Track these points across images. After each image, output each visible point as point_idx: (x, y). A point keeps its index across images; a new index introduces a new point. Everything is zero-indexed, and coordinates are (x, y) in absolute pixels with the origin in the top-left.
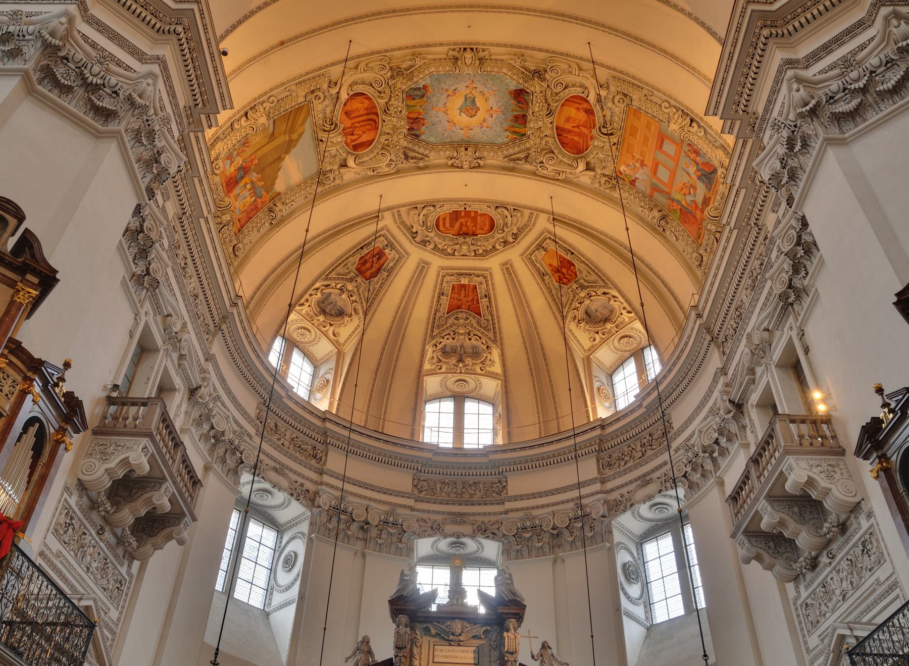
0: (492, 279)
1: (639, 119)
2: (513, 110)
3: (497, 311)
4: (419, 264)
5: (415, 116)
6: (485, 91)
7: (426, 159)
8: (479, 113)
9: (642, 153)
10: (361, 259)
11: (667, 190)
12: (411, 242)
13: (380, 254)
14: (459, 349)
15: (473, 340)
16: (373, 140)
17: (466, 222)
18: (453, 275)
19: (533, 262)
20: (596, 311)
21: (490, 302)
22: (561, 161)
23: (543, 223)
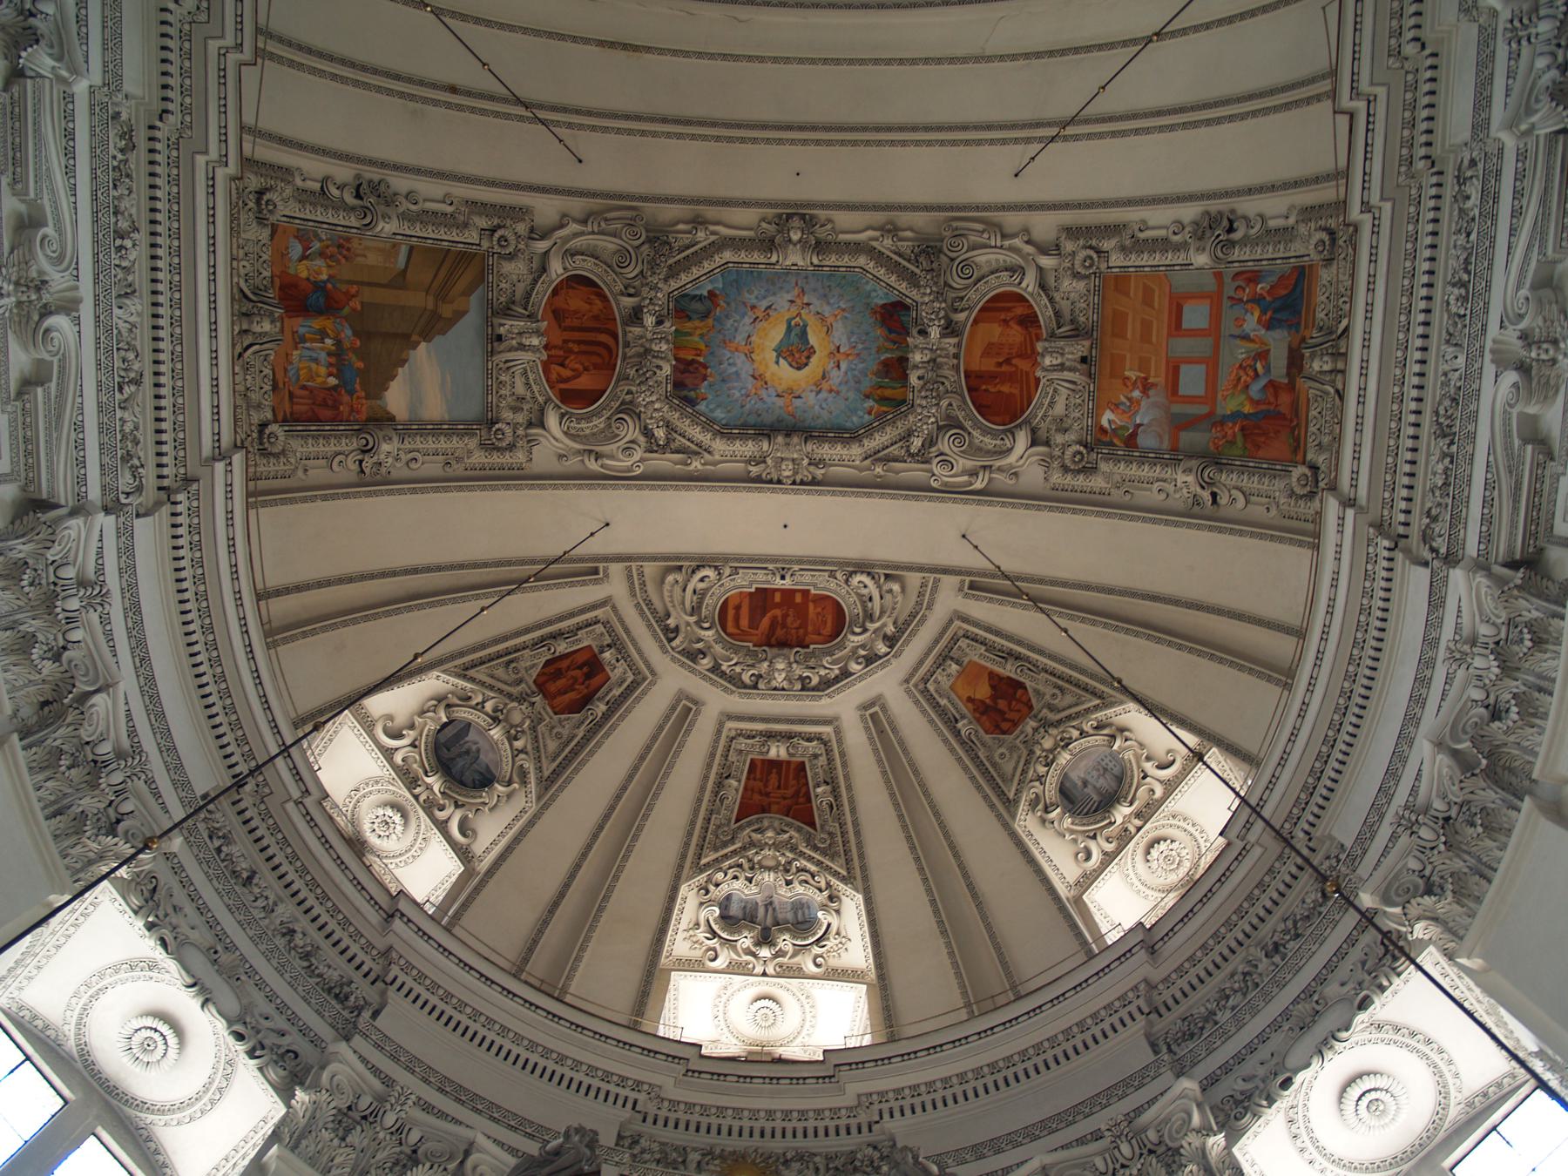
0: (840, 741)
1: (1127, 294)
2: (879, 351)
3: (853, 810)
4: (678, 701)
5: (690, 358)
6: (827, 311)
7: (707, 456)
8: (814, 360)
9: (1143, 365)
10: (548, 663)
11: (1204, 410)
12: (662, 647)
13: (592, 666)
14: (761, 911)
15: (796, 884)
16: (604, 391)
17: (785, 616)
18: (754, 737)
19: (931, 699)
20: (1085, 783)
21: (837, 797)
22: (980, 449)
23: (949, 599)
